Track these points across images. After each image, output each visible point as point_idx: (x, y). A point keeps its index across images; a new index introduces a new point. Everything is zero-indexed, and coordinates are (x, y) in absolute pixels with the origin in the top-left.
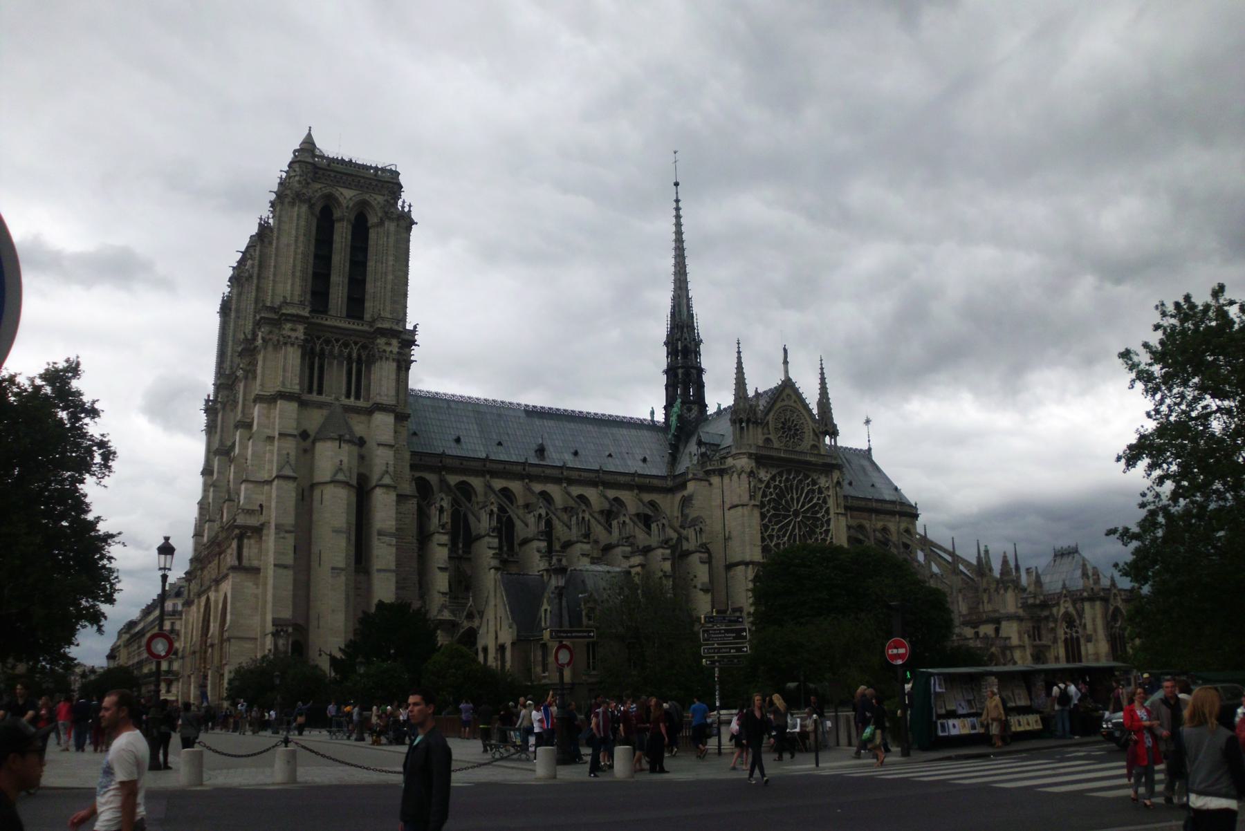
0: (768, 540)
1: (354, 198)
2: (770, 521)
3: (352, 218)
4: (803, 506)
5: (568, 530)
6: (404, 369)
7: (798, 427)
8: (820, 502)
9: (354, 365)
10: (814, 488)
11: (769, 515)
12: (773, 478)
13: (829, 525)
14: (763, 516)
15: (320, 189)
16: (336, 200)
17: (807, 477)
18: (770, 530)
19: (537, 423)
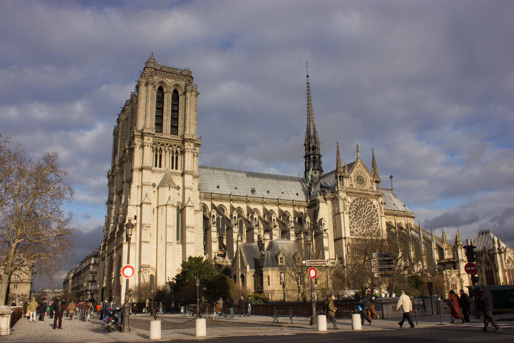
0: (353, 228)
1: (172, 83)
2: (353, 220)
3: (172, 91)
4: (367, 213)
5: (267, 225)
6: (196, 156)
7: (364, 179)
8: (374, 211)
9: (175, 155)
10: (371, 205)
11: (352, 217)
12: (354, 201)
13: (378, 221)
14: (350, 218)
15: (158, 79)
17: (368, 201)
18: (353, 224)
19: (251, 179)
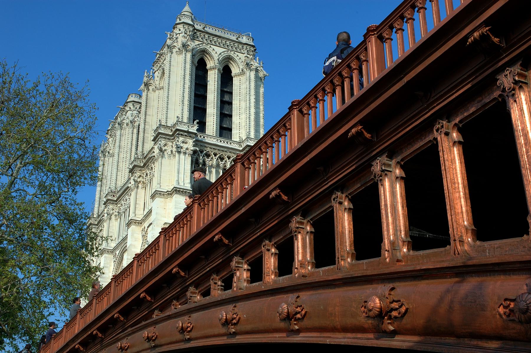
15: (198, 45)
16: (209, 54)
